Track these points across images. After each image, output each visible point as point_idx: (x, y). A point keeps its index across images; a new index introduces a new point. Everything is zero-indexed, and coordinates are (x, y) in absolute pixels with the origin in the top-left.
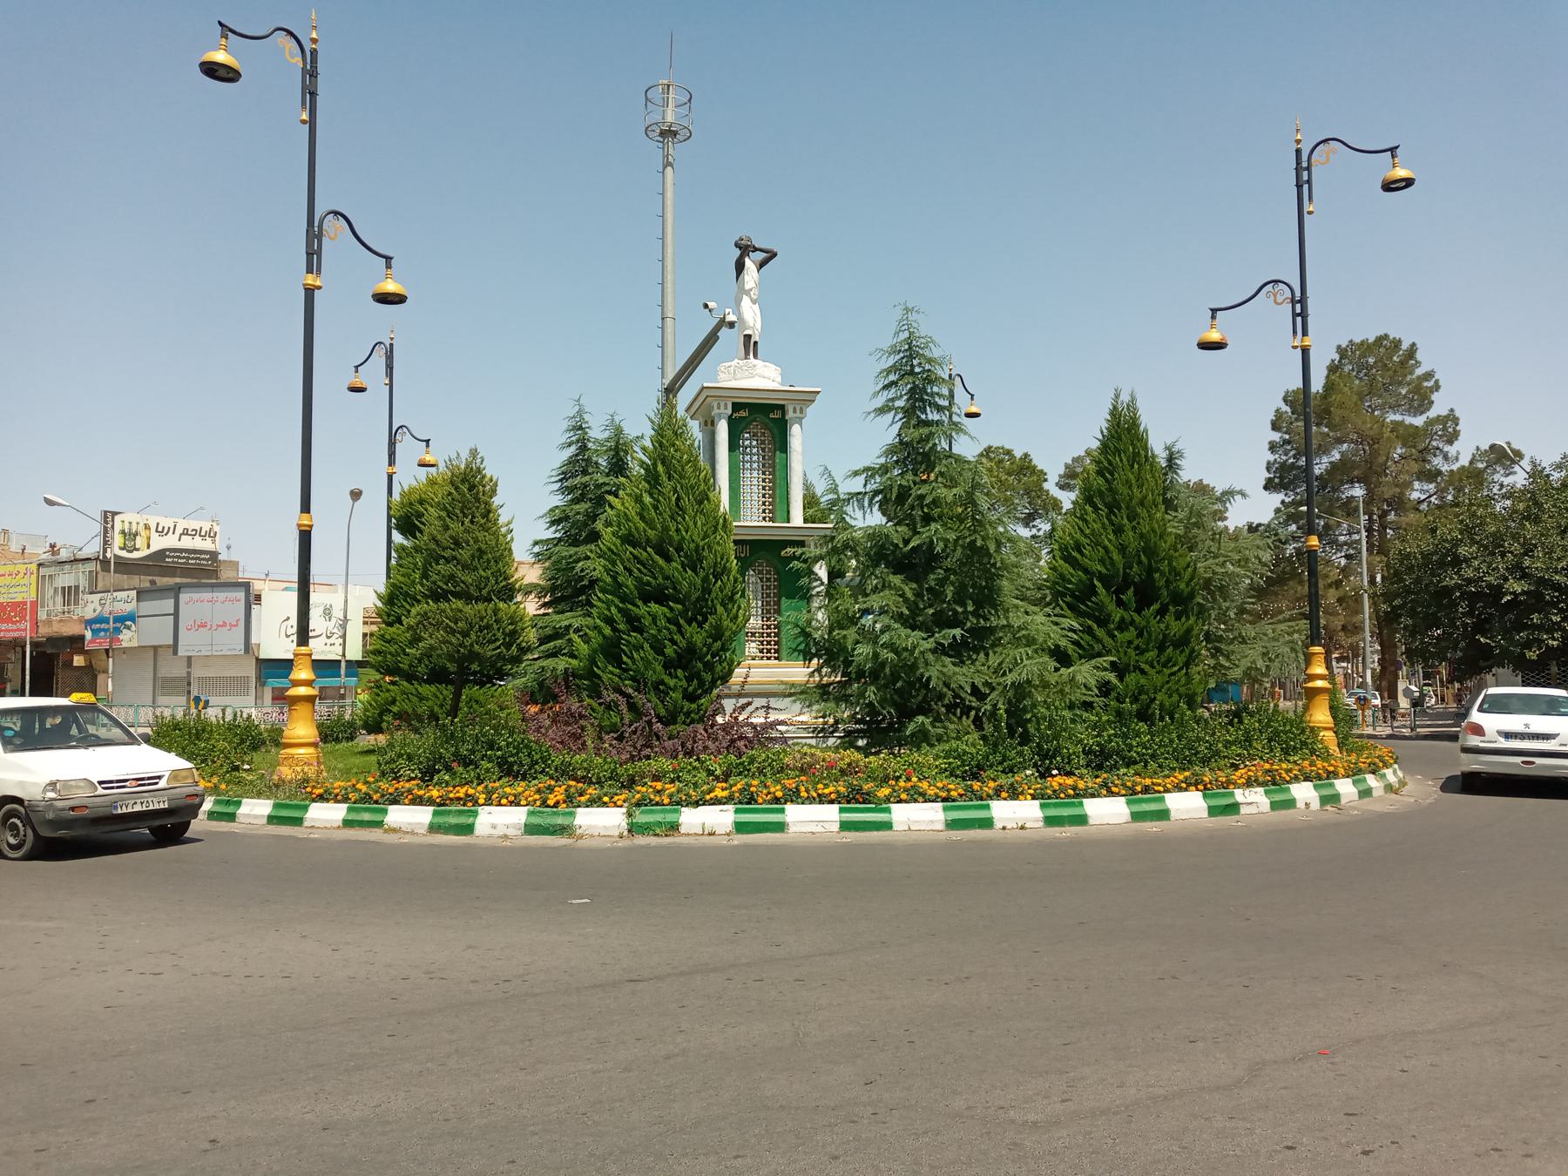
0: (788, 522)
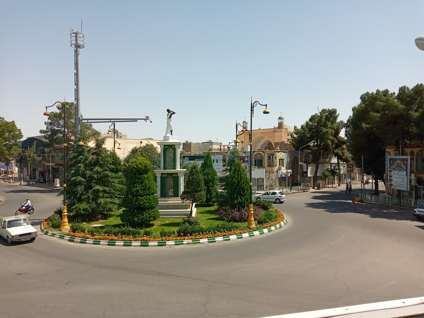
0: (175, 169)
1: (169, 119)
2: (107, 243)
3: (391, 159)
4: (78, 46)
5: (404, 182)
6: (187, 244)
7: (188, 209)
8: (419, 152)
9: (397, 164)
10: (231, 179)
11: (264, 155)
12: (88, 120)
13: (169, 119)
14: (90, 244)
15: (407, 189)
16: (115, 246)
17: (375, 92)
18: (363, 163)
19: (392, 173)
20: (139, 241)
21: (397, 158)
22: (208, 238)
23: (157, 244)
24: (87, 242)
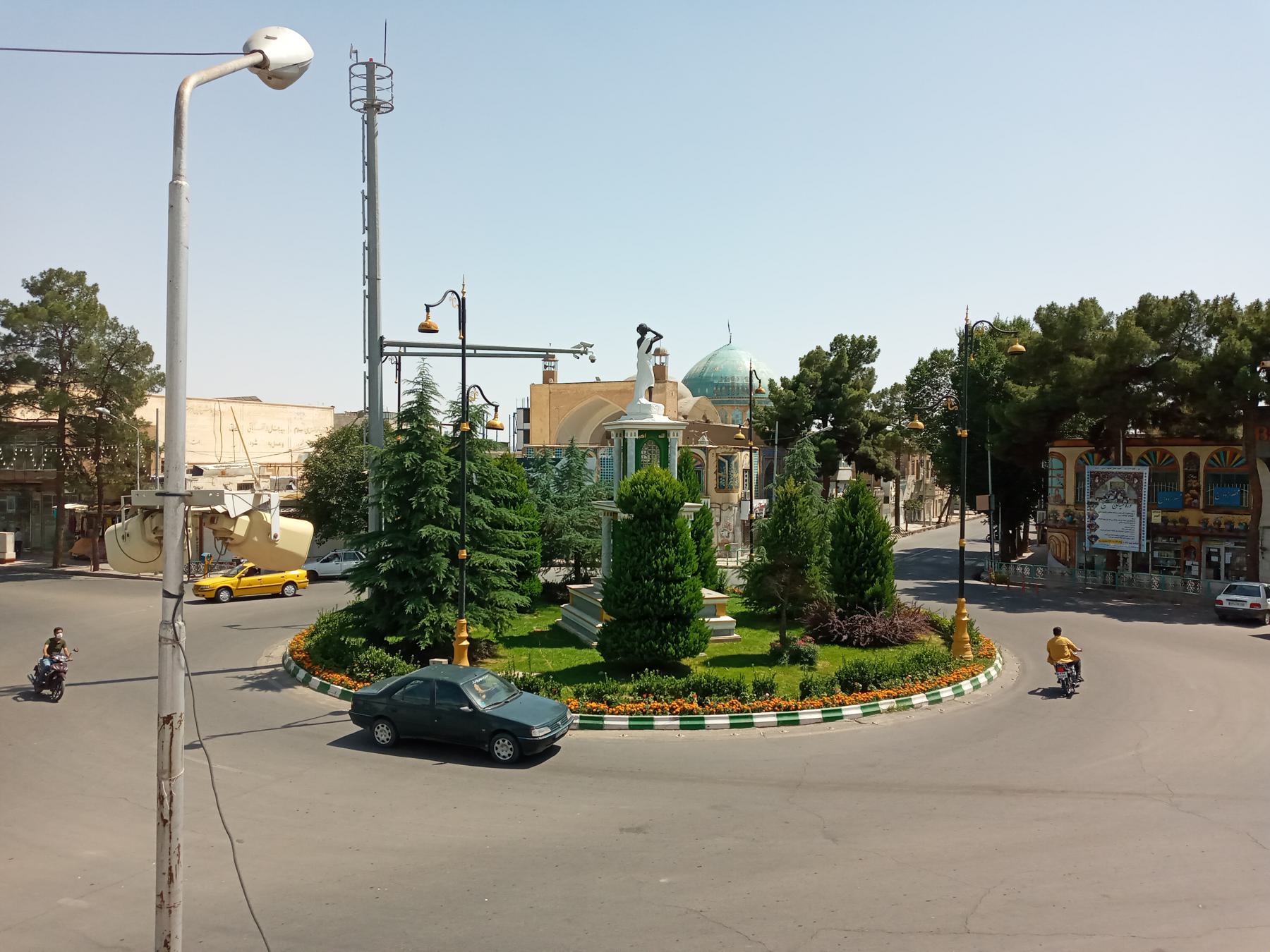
1: (647, 353)
2: (678, 723)
3: (1094, 475)
4: (372, 107)
5: (1131, 530)
6: (890, 710)
7: (719, 617)
8: (1145, 456)
9: (1111, 486)
10: (848, 530)
11: (707, 459)
12: (407, 348)
13: (647, 353)
14: (620, 728)
15: (1140, 548)
16: (704, 728)
17: (1076, 304)
18: (992, 482)
19: (1098, 509)
20: (769, 711)
21: (1113, 473)
22: (924, 692)
23: (820, 716)
24: (605, 722)
